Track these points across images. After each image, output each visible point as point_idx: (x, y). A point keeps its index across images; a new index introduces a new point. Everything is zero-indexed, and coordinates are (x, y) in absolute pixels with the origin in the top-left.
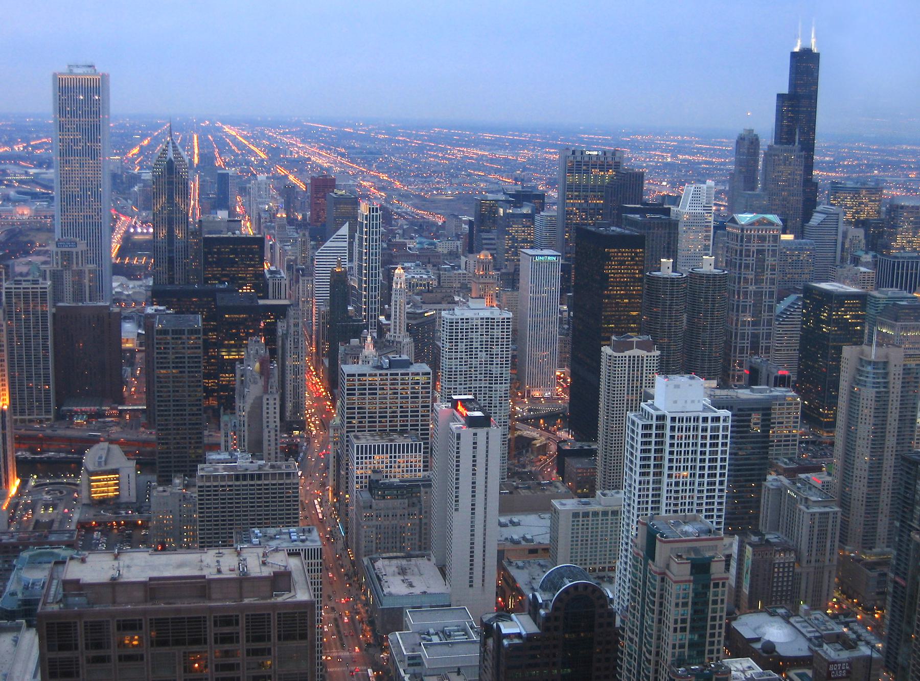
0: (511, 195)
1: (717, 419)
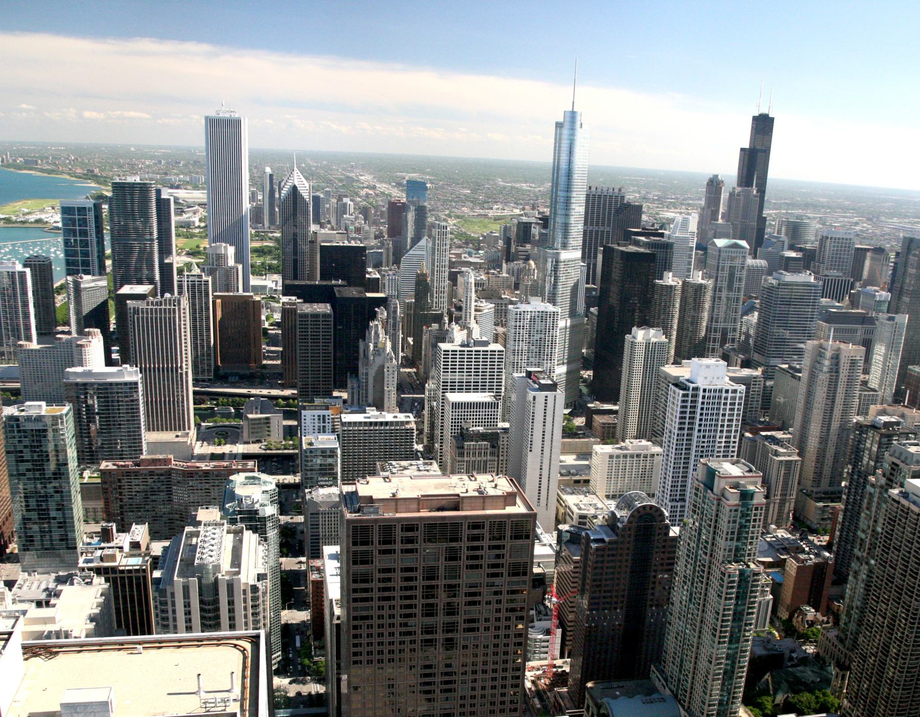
0: (540, 219)
1: (735, 391)
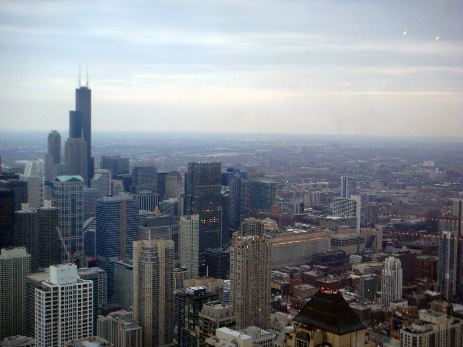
1: (85, 286)
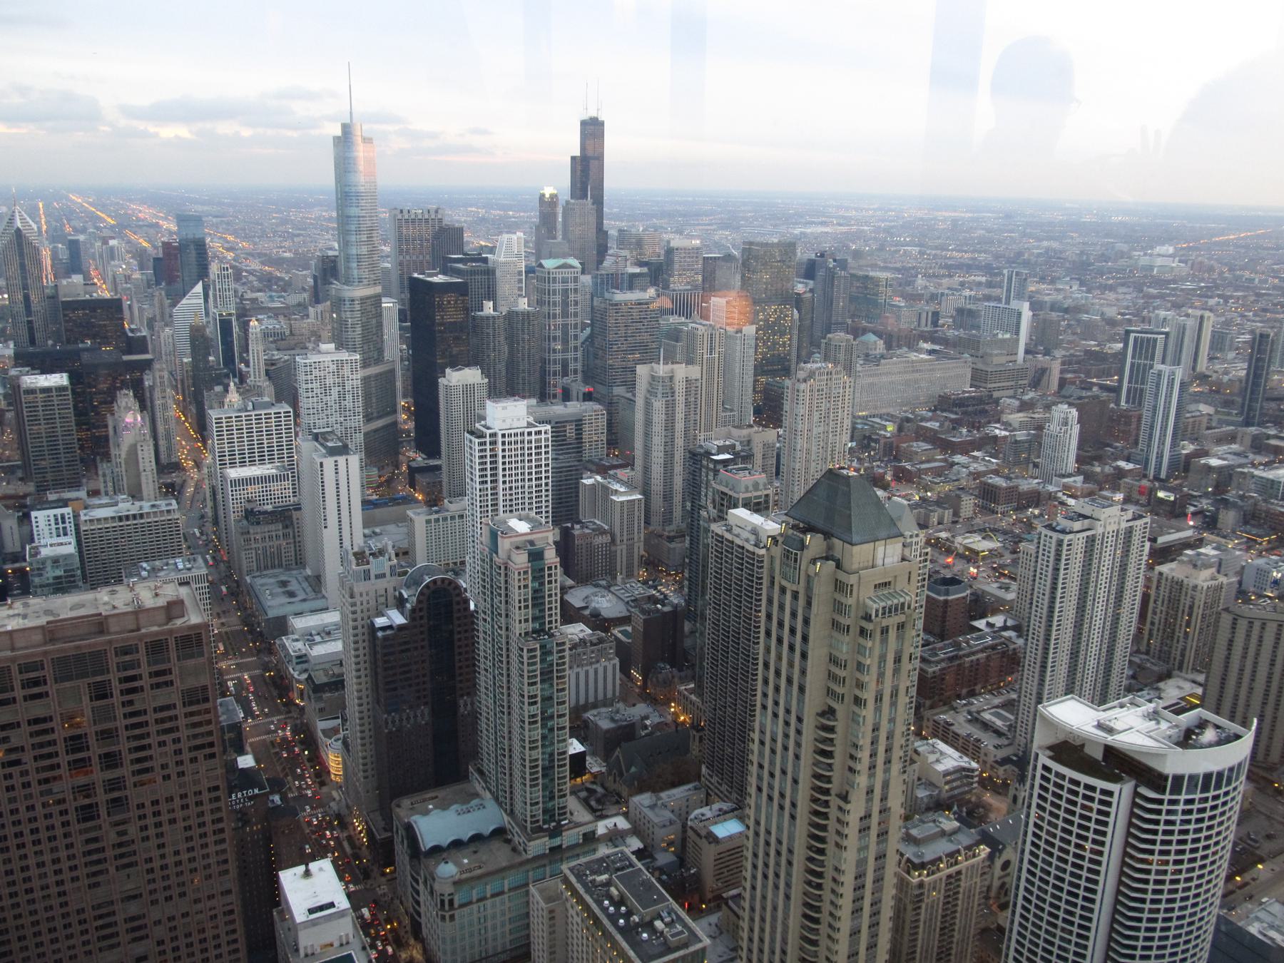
1: (539, 433)
